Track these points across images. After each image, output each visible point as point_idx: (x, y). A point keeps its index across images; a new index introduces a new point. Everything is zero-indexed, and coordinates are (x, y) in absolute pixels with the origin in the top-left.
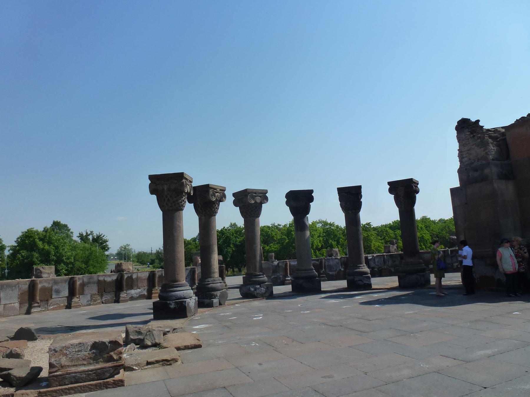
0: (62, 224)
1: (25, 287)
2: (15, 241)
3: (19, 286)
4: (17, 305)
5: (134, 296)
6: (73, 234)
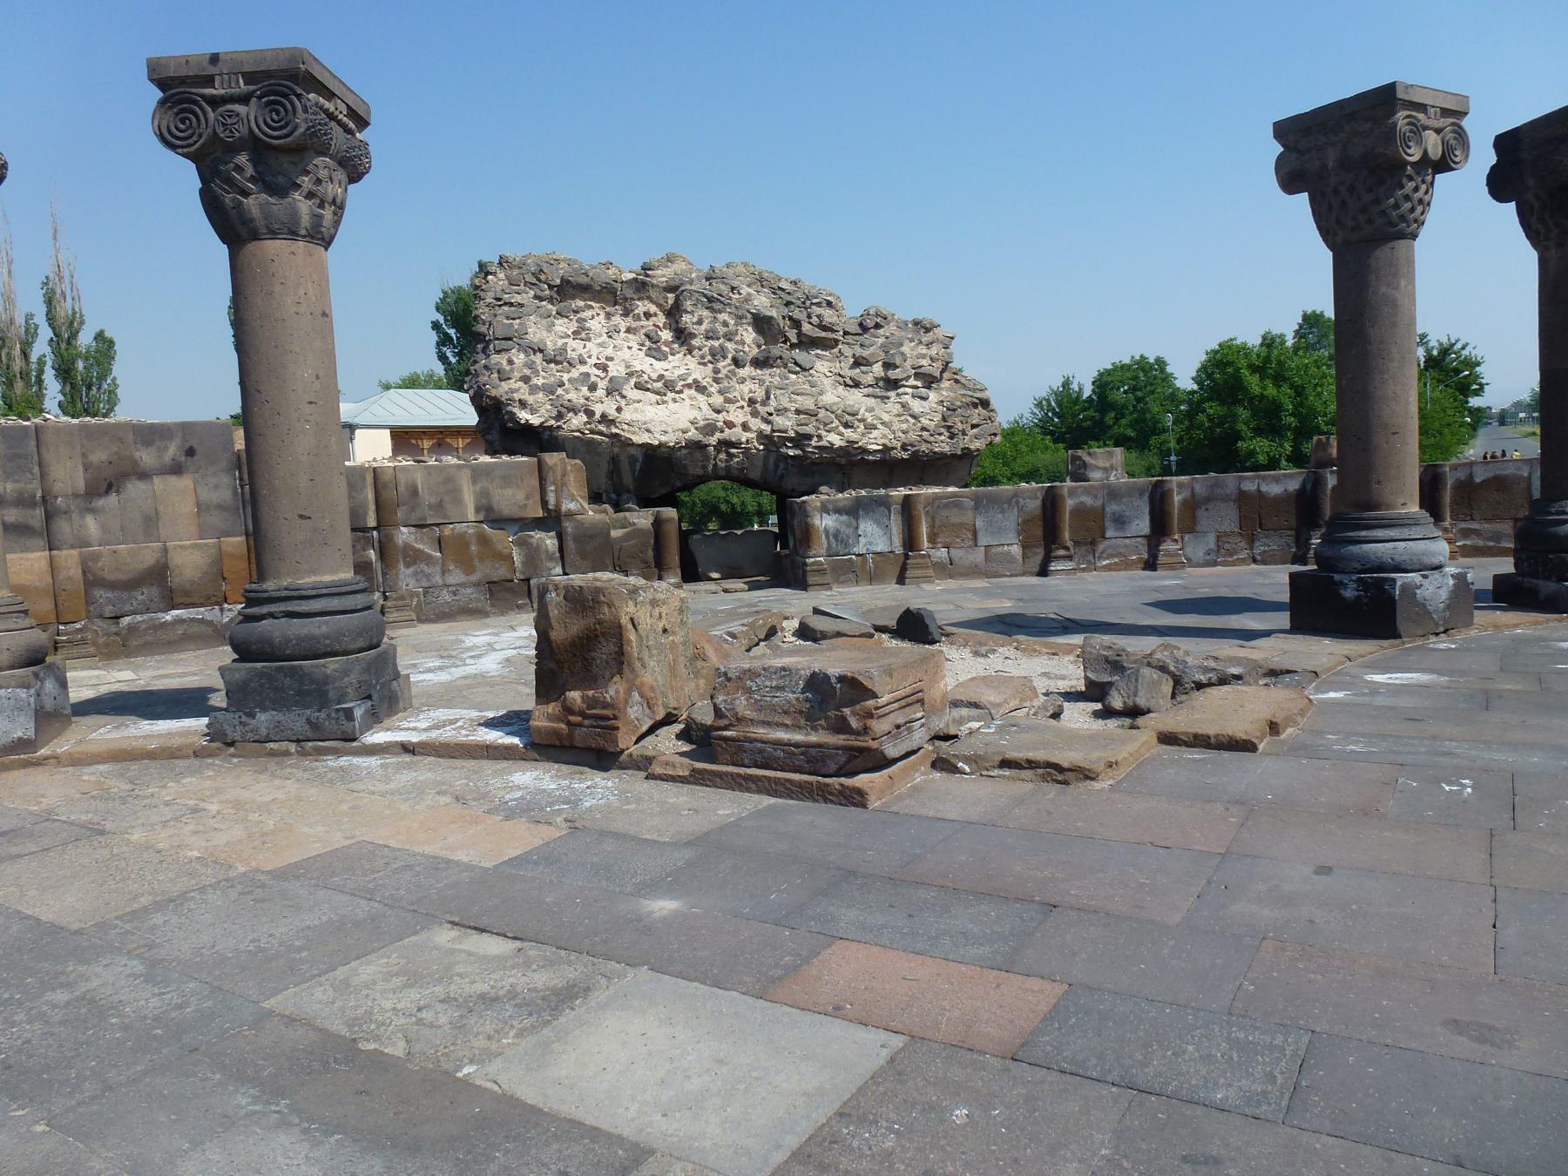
1: (1034, 505)
2: (1193, 379)
3: (1017, 503)
4: (1016, 550)
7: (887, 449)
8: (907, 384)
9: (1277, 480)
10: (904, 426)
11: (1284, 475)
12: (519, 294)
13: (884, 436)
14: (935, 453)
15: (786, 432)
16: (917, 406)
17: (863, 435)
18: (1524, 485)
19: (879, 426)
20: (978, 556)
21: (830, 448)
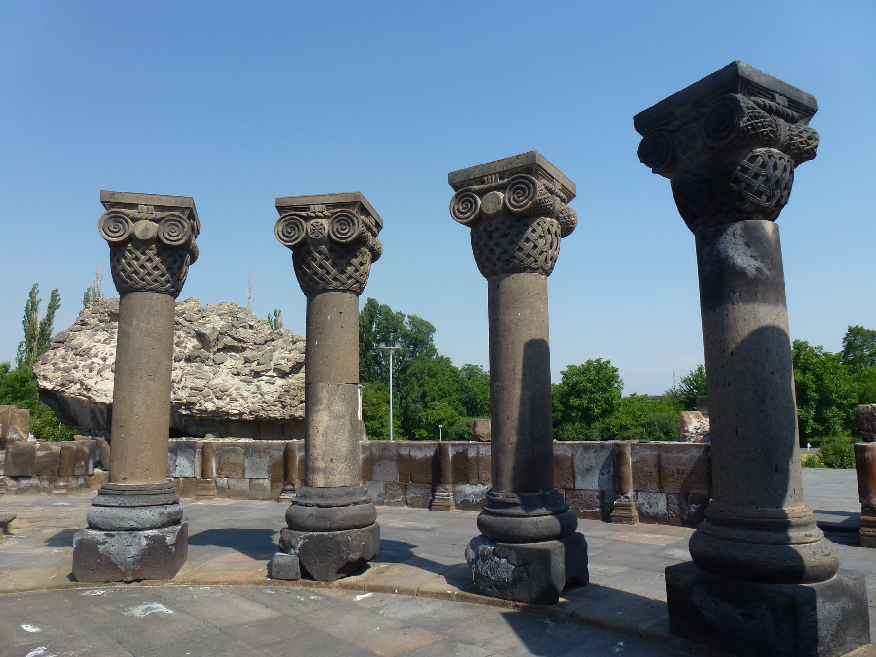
0: (868, 331)
1: (279, 454)
3: (269, 452)
4: (267, 483)
5: (471, 501)
7: (241, 414)
8: (267, 374)
9: (420, 447)
10: (254, 400)
11: (425, 445)
12: (93, 318)
13: (241, 405)
14: (270, 417)
15: (181, 400)
16: (266, 388)
17: (228, 404)
18: (568, 464)
19: (241, 399)
20: (244, 485)
21: (206, 411)
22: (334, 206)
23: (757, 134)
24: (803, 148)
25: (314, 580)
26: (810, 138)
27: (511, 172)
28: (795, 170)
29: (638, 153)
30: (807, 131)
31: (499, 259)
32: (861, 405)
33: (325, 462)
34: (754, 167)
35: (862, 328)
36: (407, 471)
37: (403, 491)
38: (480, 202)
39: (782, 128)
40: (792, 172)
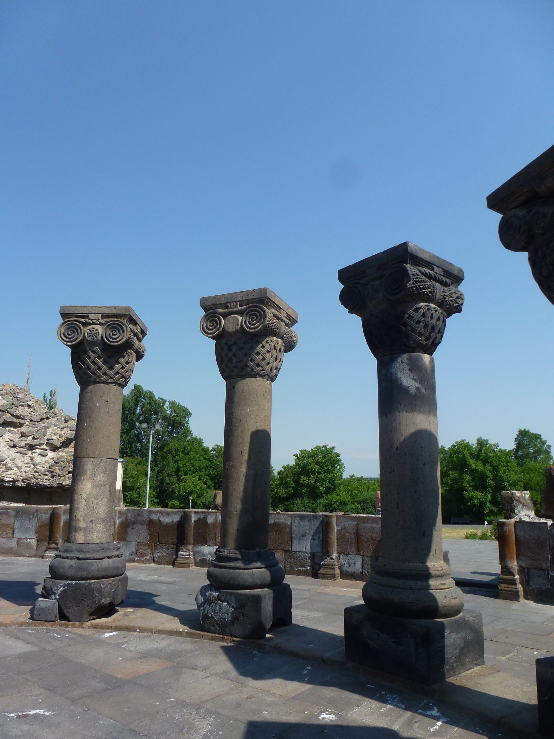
0: (533, 434)
1: (46, 517)
3: (38, 515)
4: (33, 542)
5: (208, 559)
6: (551, 448)
7: (14, 481)
8: (40, 447)
9: (168, 514)
10: (27, 469)
11: (172, 512)
13: (15, 474)
16: (38, 459)
17: (3, 472)
18: (288, 530)
19: (15, 469)
20: (13, 543)
22: (108, 316)
23: (420, 293)
24: (453, 304)
25: (70, 621)
26: (458, 298)
27: (248, 302)
28: (447, 320)
29: (340, 299)
30: (456, 293)
31: (235, 367)
32: (503, 491)
33: (86, 523)
34: (417, 316)
35: (528, 431)
36: (156, 533)
37: (152, 550)
38: (223, 322)
39: (438, 290)
40: (444, 321)
